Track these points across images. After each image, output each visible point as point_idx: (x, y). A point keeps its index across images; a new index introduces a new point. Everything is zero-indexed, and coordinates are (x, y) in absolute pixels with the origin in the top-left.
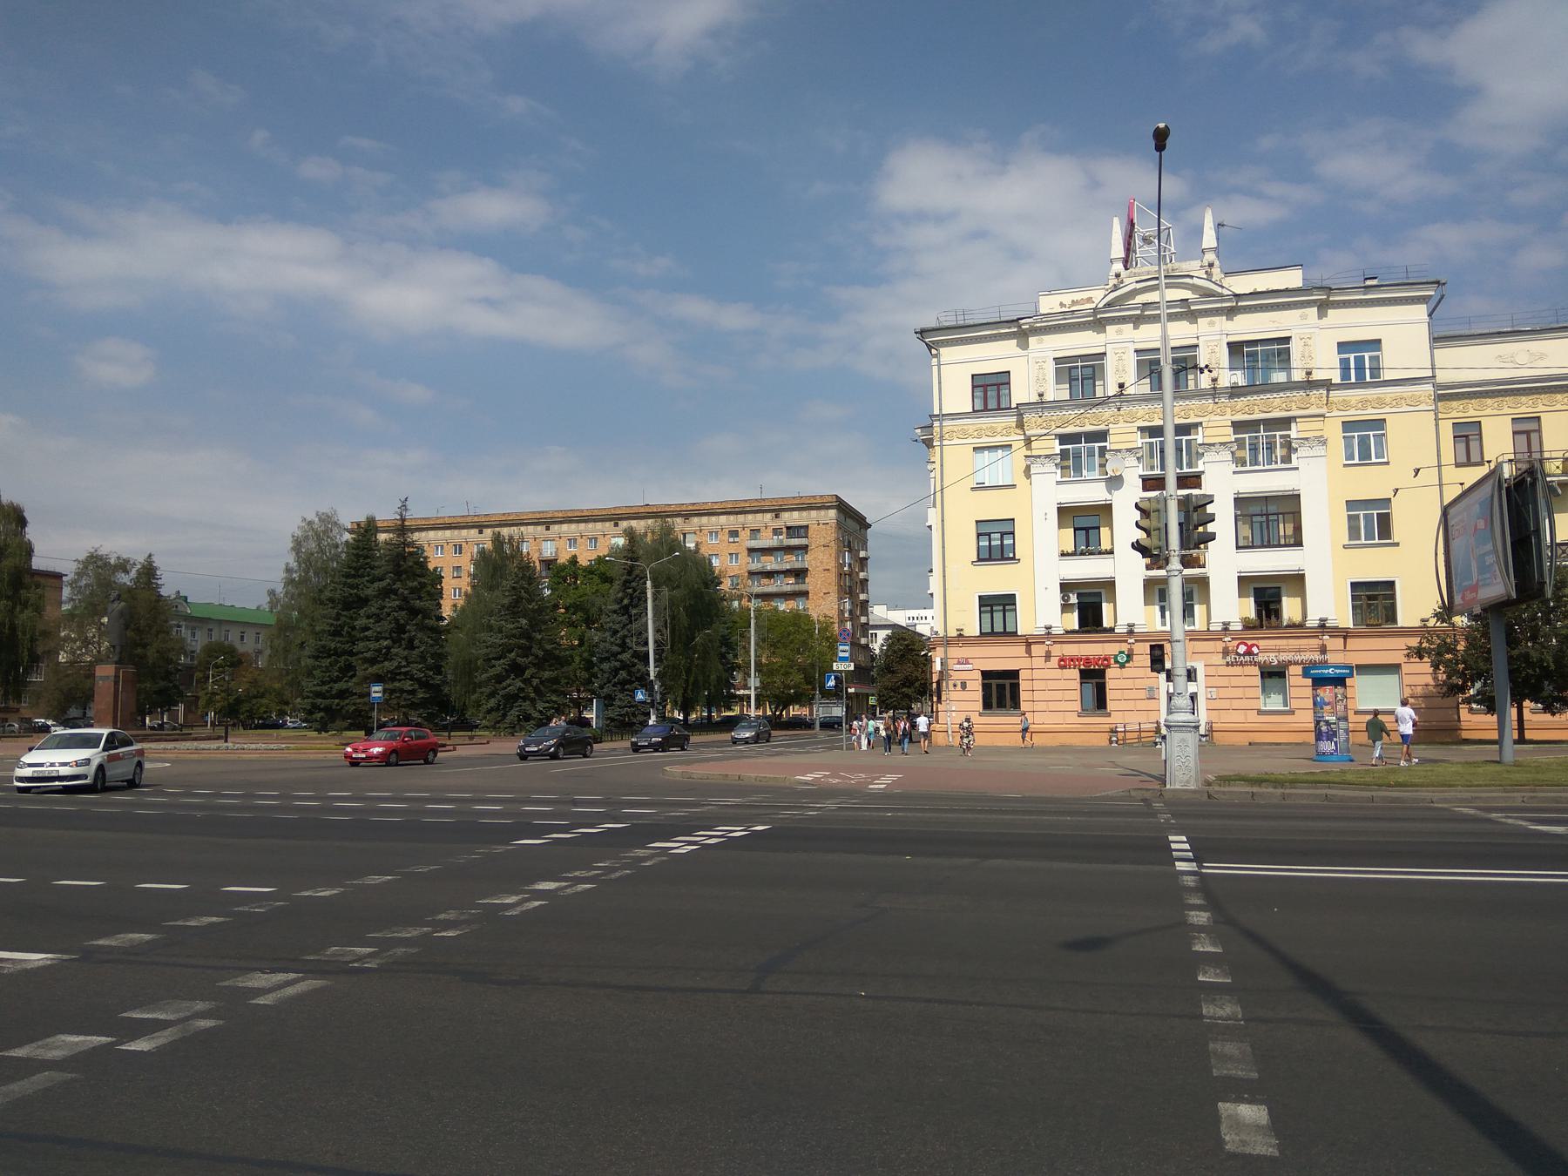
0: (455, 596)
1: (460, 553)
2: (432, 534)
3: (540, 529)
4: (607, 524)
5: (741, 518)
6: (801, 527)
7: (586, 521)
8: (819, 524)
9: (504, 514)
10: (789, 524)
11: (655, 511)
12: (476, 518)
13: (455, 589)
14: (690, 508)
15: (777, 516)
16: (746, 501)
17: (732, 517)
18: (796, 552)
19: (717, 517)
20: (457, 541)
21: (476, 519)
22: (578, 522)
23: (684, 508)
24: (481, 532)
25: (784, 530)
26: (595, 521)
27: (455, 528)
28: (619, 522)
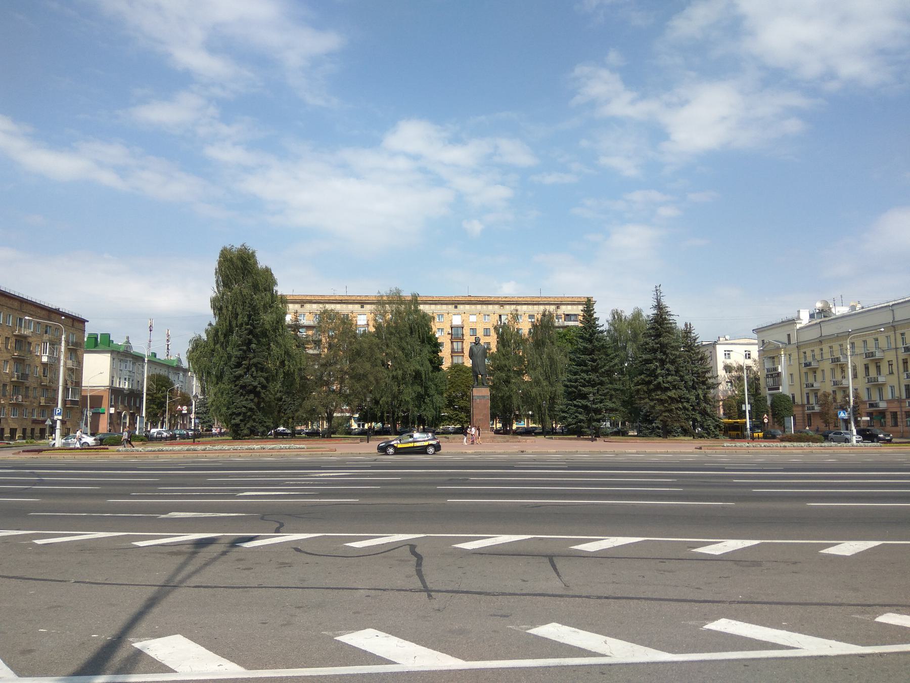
2: (525, 307)
3: (451, 307)
4: (450, 306)
7: (436, 304)
10: (566, 313)
11: (481, 300)
12: (359, 297)
14: (504, 299)
16: (550, 297)
17: (530, 307)
21: (359, 298)
22: (431, 304)
23: (500, 299)
24: (362, 307)
25: (563, 316)
26: (442, 304)
27: (344, 303)
28: (458, 306)
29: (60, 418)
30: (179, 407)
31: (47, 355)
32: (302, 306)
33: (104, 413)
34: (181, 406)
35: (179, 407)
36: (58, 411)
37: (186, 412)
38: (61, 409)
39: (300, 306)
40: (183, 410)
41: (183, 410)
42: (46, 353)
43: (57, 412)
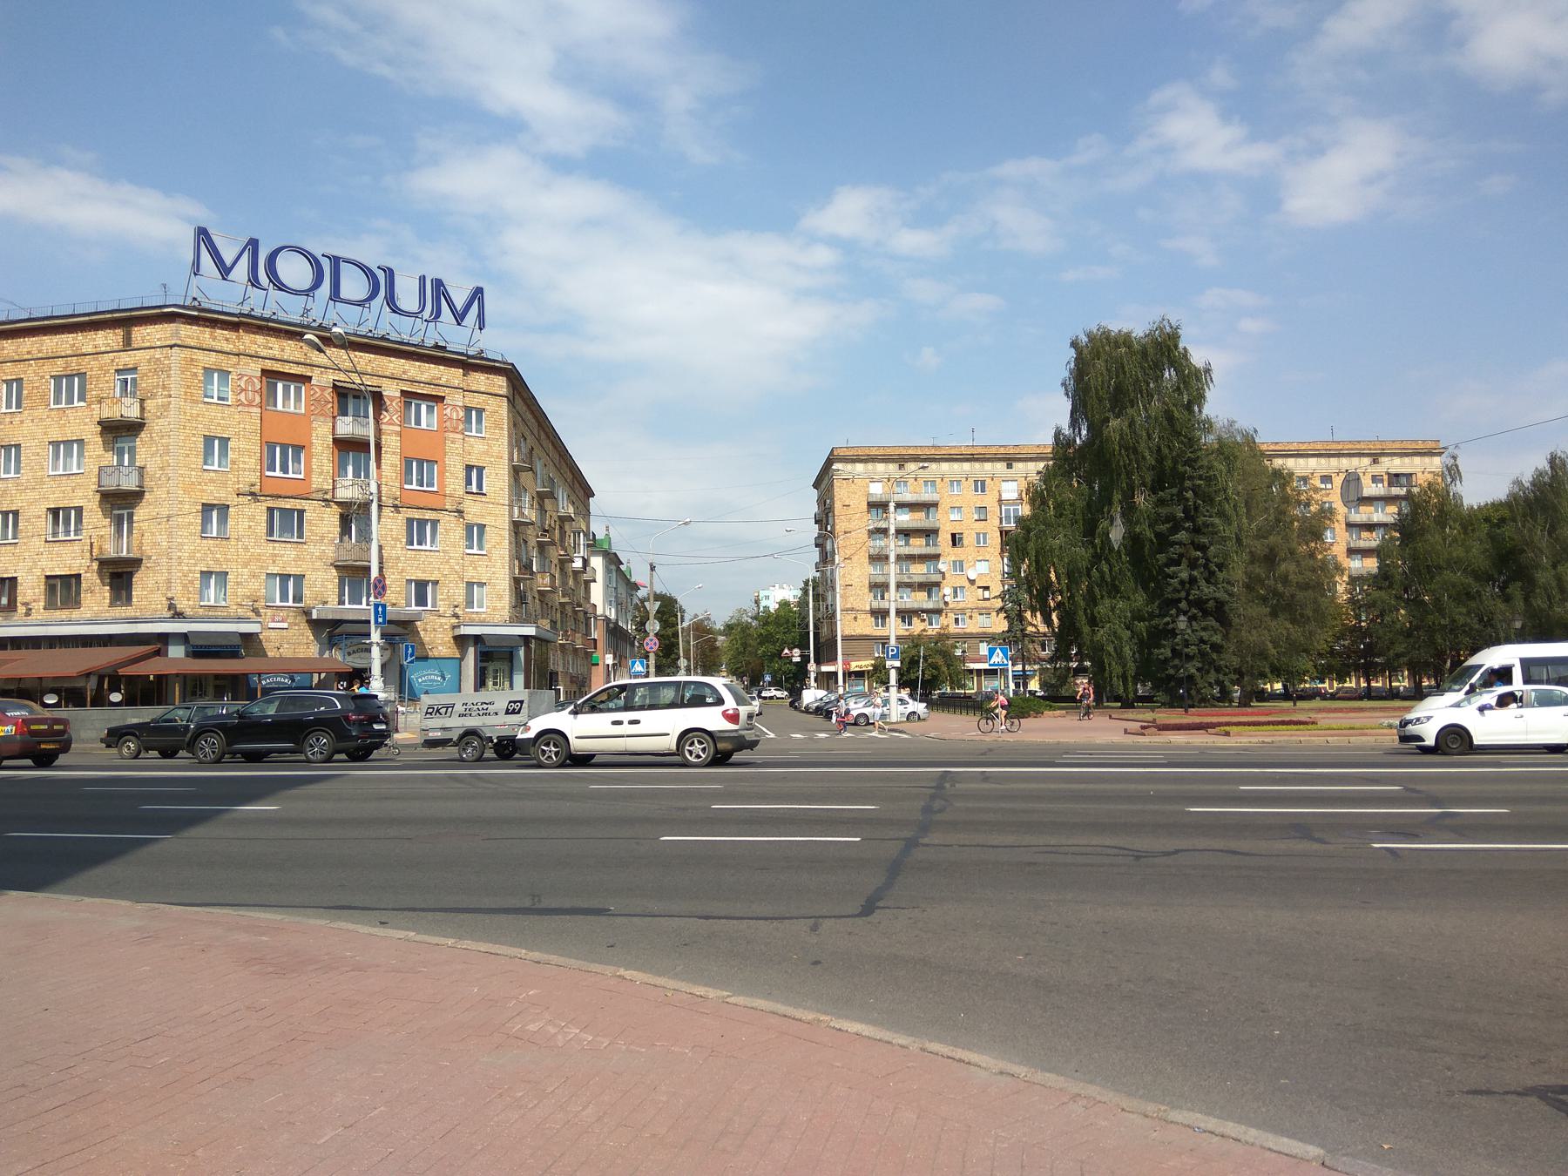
0: (978, 542)
1: (983, 491)
5: (1334, 461)
6: (1404, 475)
8: (1423, 473)
9: (1038, 446)
10: (1393, 471)
12: (1002, 449)
13: (978, 534)
15: (1375, 462)
17: (1323, 461)
18: (1375, 503)
19: (1305, 459)
20: (980, 477)
21: (1002, 450)
24: (1009, 466)
25: (1386, 477)
27: (977, 460)
29: (897, 664)
30: (786, 651)
31: (582, 554)
32: (901, 467)
33: (598, 664)
34: (789, 649)
35: (786, 651)
36: (893, 651)
37: (798, 659)
38: (897, 648)
39: (898, 467)
40: (793, 656)
41: (793, 656)
42: (579, 553)
43: (890, 653)
